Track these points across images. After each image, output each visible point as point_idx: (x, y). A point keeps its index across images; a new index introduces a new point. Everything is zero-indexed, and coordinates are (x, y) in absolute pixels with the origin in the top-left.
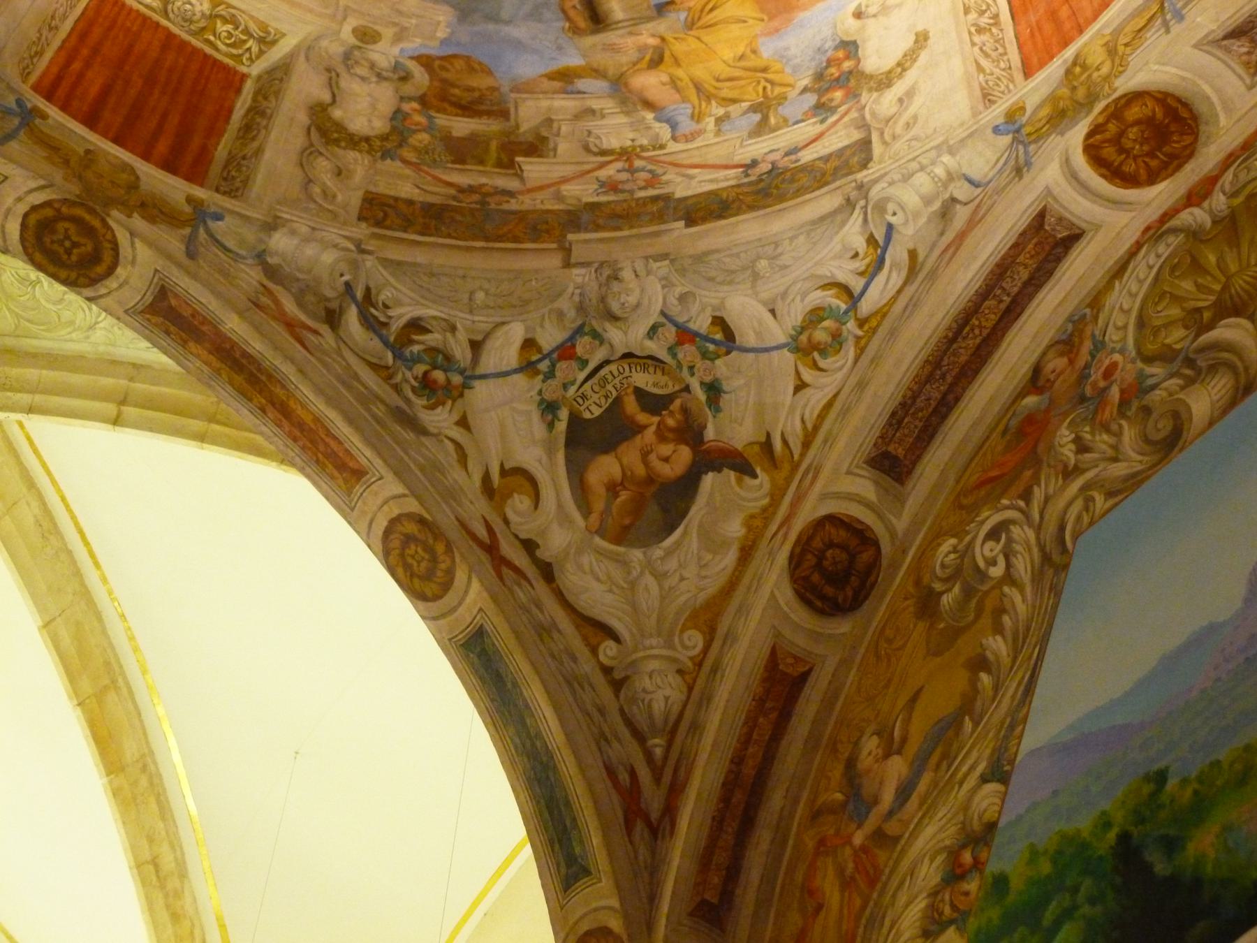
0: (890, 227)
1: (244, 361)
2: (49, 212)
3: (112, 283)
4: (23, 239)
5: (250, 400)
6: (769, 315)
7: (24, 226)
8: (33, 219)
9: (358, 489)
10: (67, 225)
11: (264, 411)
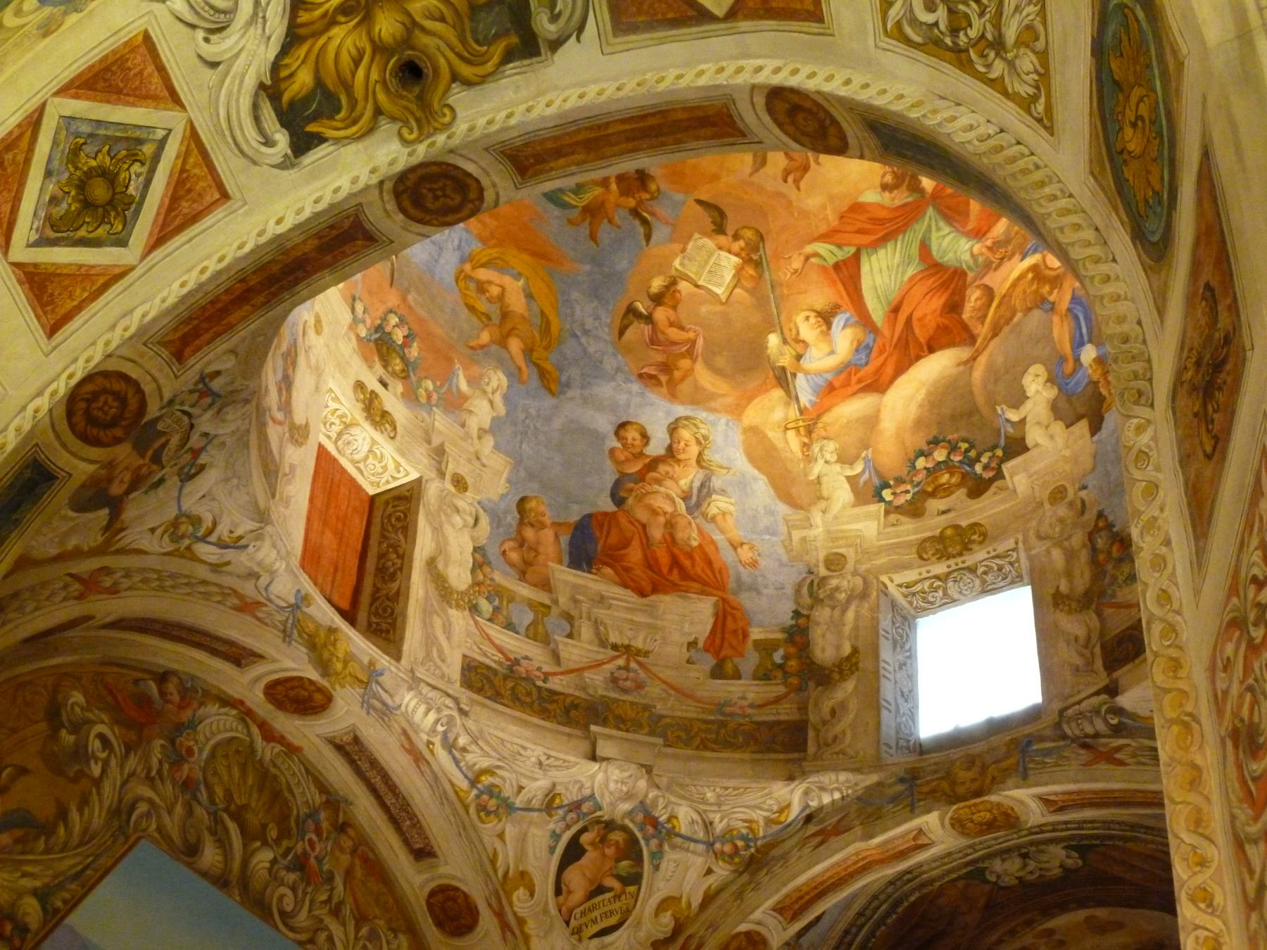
0: (246, 547)
1: (291, 278)
2: (472, 195)
3: (391, 206)
4: (456, 167)
5: (254, 273)
6: (201, 494)
7: (470, 175)
8: (469, 181)
9: (165, 353)
10: (458, 199)
11: (243, 281)
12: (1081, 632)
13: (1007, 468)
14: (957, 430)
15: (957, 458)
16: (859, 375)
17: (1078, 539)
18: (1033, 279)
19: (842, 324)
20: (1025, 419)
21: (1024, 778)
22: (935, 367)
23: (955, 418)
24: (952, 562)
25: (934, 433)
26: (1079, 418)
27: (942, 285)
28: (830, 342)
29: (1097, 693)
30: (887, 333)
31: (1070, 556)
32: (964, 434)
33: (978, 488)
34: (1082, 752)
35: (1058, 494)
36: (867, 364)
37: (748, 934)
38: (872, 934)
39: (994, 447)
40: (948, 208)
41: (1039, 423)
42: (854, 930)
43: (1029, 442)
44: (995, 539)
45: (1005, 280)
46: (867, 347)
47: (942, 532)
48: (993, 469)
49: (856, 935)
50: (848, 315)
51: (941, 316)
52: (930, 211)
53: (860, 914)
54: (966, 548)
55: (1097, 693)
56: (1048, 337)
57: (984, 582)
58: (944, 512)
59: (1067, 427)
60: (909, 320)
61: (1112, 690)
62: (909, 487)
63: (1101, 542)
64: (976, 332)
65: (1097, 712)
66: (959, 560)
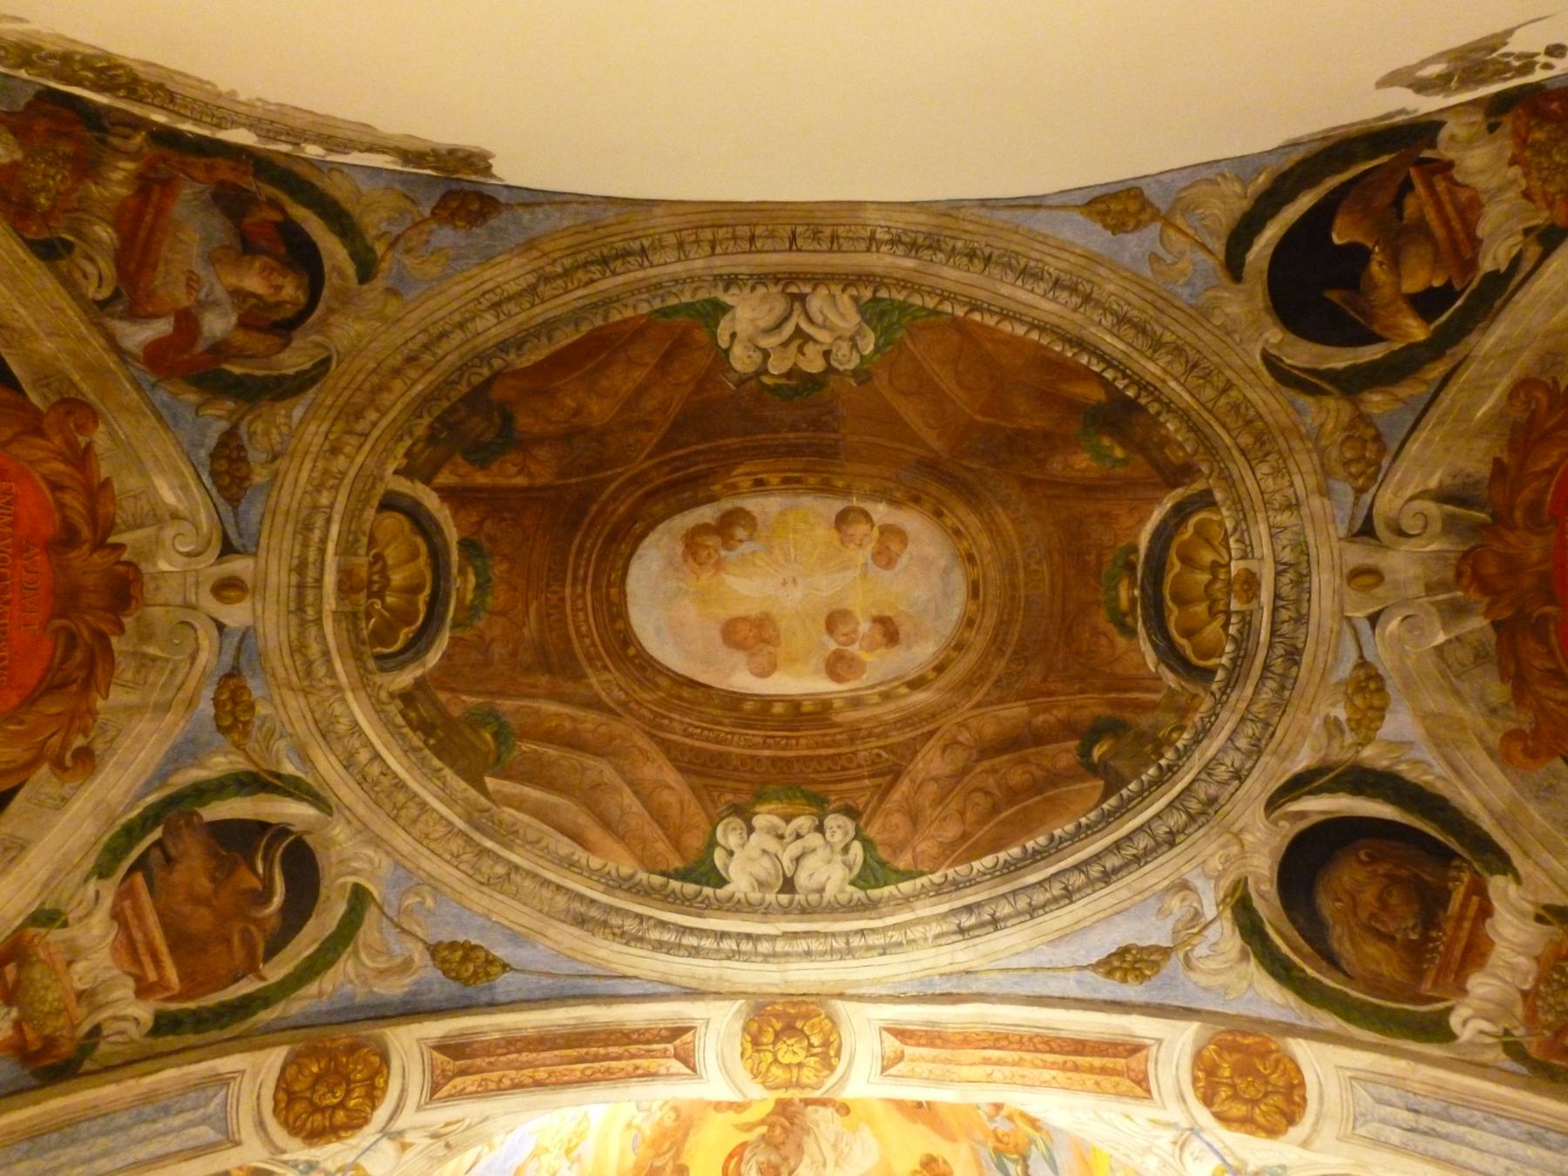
37: (1208, 1101)
38: (1082, 833)
42: (1095, 870)
49: (1097, 857)
53: (1069, 895)
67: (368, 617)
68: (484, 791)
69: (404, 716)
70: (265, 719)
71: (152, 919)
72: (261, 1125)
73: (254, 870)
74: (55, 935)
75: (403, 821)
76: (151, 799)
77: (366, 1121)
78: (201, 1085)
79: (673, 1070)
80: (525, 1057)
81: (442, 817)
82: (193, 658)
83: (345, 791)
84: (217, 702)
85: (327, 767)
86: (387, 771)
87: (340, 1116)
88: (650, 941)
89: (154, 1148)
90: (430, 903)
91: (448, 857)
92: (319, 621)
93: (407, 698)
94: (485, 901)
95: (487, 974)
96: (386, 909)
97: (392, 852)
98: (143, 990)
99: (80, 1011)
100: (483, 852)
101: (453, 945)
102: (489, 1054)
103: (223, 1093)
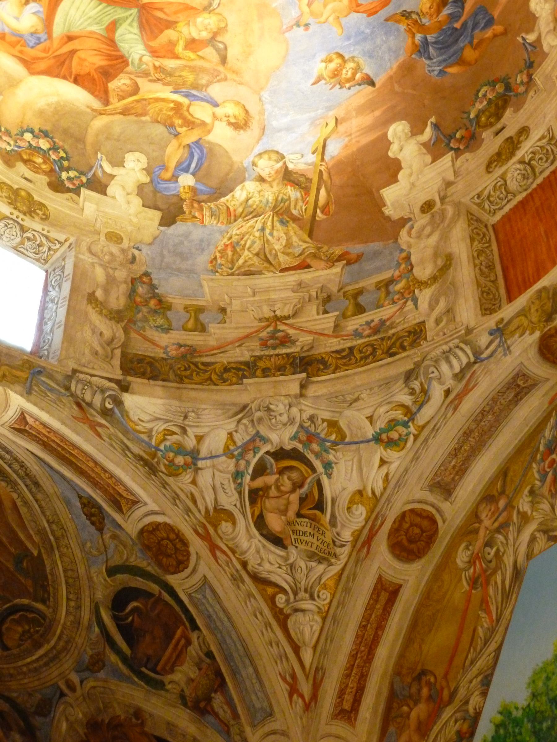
12: (108, 334)
13: (83, 191)
14: (64, 141)
15: (53, 157)
16: (23, 48)
17: (121, 274)
18: (172, 109)
19: (34, 10)
20: (114, 176)
21: (28, 393)
22: (76, 96)
23: (66, 132)
24: (16, 213)
25: (48, 127)
26: (157, 208)
27: (110, 55)
28: (21, 12)
29: (110, 380)
30: (56, 44)
31: (111, 281)
32: (66, 147)
33: (57, 186)
34: (74, 407)
35: (114, 237)
36: (32, 47)
39: (82, 173)
40: (147, 21)
41: (123, 188)
43: (109, 190)
44: (53, 225)
45: (150, 91)
46: (39, 39)
47: (17, 189)
48: (74, 184)
50: (41, 9)
51: (96, 70)
52: (134, 11)
54: (30, 213)
55: (110, 380)
56: (163, 148)
57: (22, 243)
58: (26, 179)
59: (143, 206)
60: (73, 52)
61: (125, 388)
62: (12, 143)
63: (141, 290)
64: (111, 100)
65: (103, 391)
66: (21, 216)
67: (38, 632)
68: (40, 553)
69: (49, 599)
70: (91, 649)
71: (167, 653)
72: (194, 571)
73: (133, 619)
74: (187, 693)
75: (76, 574)
76: (136, 679)
77: (166, 524)
78: (196, 606)
79: (33, 420)
80: (93, 475)
81: (62, 562)
82: (94, 687)
83: (86, 603)
84: (99, 671)
85: (86, 615)
86: (68, 592)
87: (172, 536)
88: (12, 456)
89: (221, 615)
90: (89, 545)
91: (70, 550)
92: (54, 647)
93: (44, 601)
94: (69, 524)
95: (89, 502)
96: (105, 559)
97: (88, 572)
98: (189, 642)
99: (204, 666)
100: (57, 539)
101: (93, 523)
102: (106, 490)
103: (193, 595)
